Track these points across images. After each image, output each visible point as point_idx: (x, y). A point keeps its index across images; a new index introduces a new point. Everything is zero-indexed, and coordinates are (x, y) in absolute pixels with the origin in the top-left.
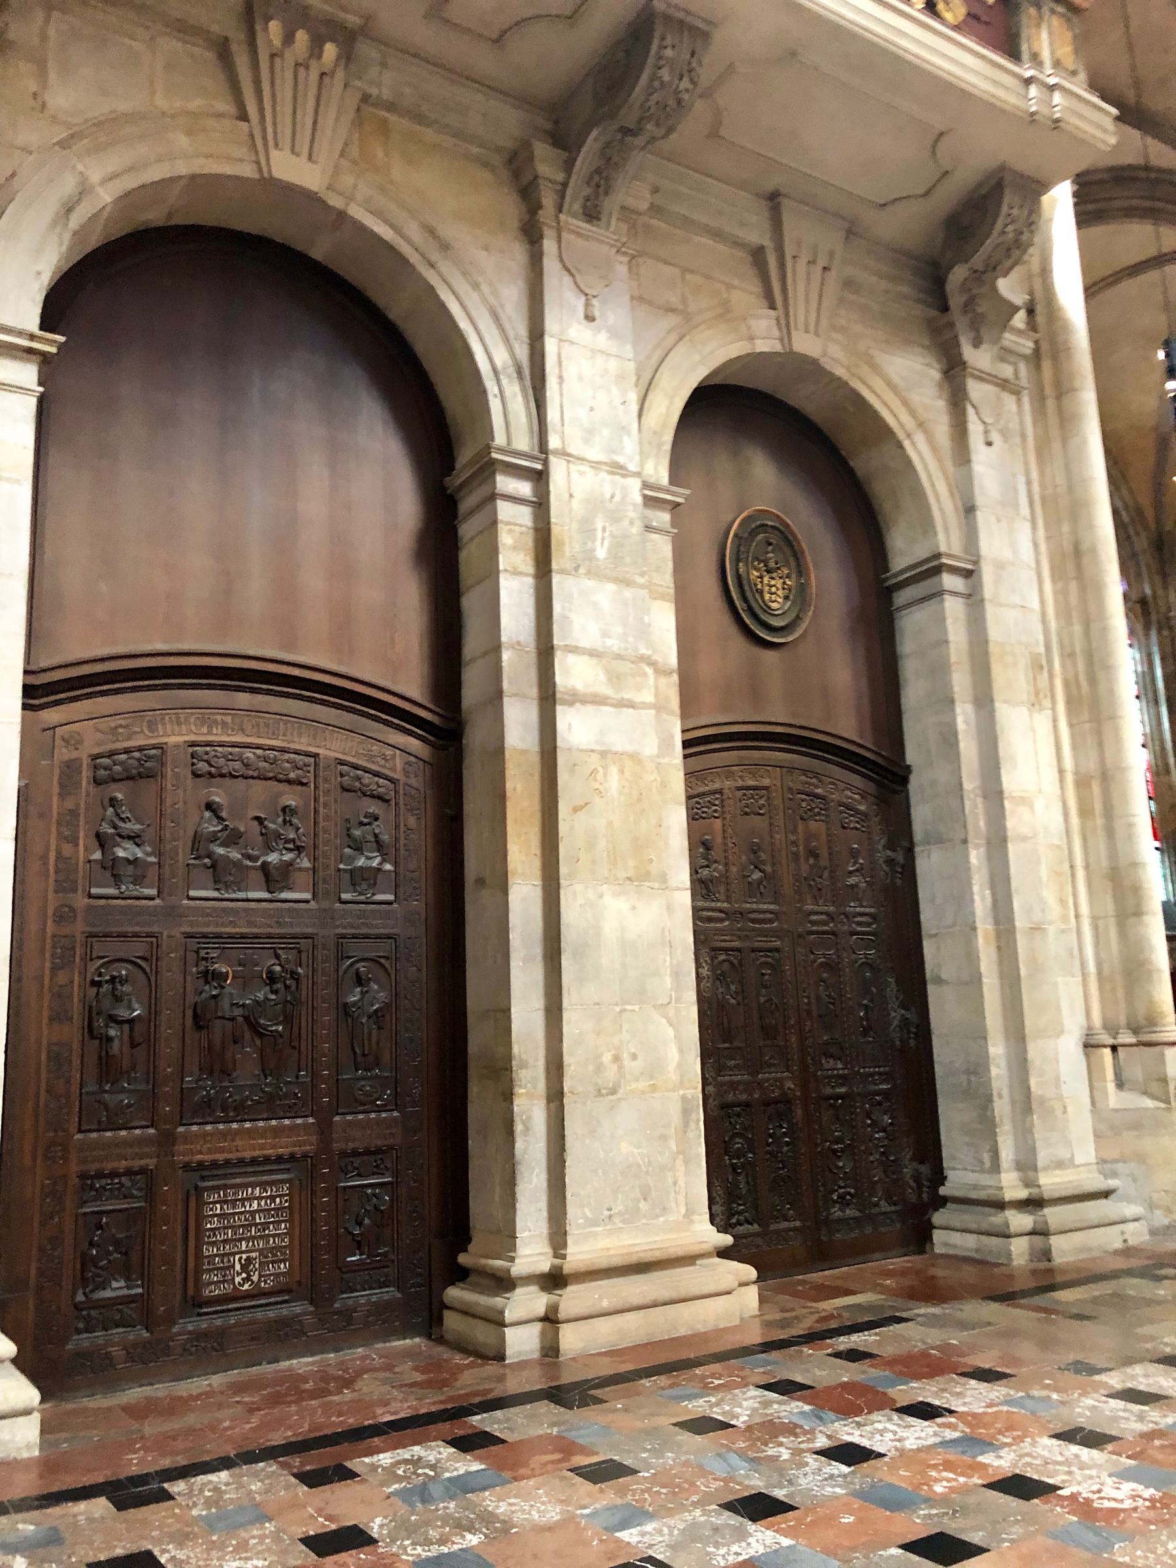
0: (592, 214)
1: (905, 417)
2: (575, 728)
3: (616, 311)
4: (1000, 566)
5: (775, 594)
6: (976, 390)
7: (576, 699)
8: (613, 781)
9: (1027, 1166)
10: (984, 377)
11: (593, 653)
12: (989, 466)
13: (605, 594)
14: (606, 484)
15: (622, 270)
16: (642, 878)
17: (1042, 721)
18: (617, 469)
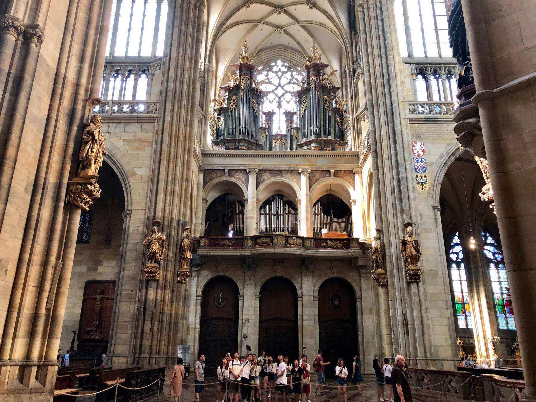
0: (307, 270)
1: (352, 281)
2: (305, 323)
3: (310, 279)
4: (365, 297)
5: (336, 303)
6: (362, 275)
7: (305, 320)
8: (309, 328)
9: (364, 370)
10: (364, 273)
11: (307, 315)
12: (364, 285)
13: (309, 309)
14: (309, 298)
15: (311, 274)
16: (312, 337)
17: (371, 317)
18: (310, 296)
